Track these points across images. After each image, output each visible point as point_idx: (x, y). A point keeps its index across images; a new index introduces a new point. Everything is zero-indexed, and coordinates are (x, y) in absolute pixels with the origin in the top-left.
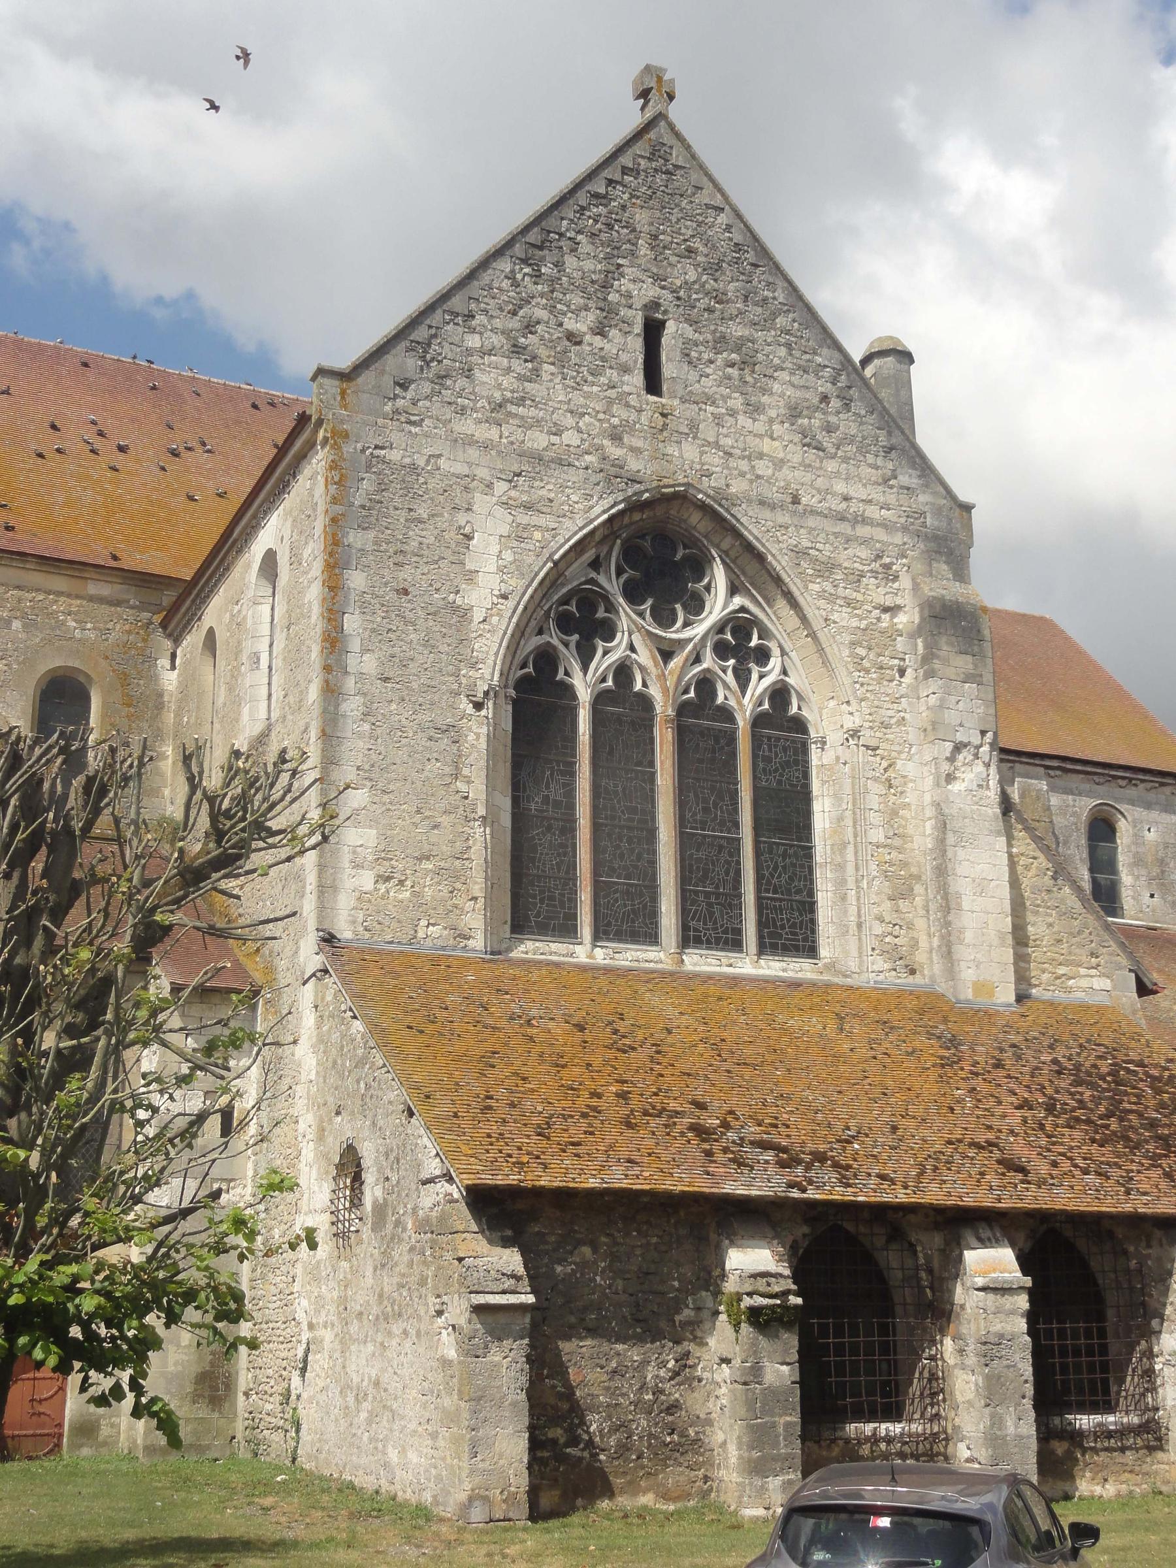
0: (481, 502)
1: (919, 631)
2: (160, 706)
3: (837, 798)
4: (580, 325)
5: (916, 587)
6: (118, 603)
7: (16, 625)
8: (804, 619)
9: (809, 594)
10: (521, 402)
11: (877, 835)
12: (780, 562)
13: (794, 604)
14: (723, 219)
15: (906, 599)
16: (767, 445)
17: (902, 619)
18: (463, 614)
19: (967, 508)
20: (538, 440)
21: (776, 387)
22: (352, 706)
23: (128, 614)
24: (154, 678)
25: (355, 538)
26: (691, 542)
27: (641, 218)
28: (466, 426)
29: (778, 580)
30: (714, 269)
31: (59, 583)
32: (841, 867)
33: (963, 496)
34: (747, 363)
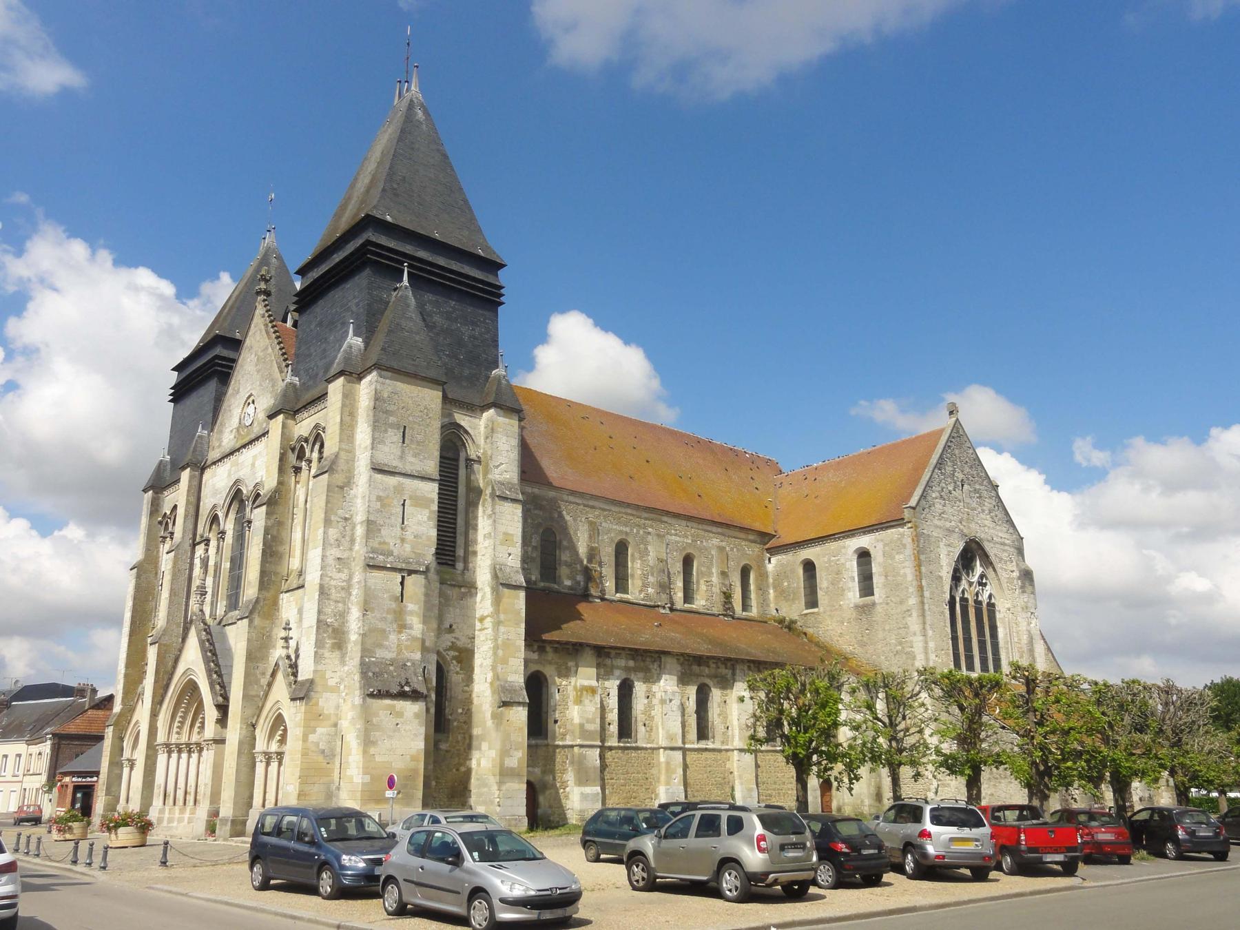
0: (942, 545)
1: (1019, 578)
2: (767, 577)
3: (1005, 628)
4: (951, 488)
5: (1017, 565)
6: (754, 542)
7: (735, 550)
8: (997, 575)
9: (998, 566)
10: (943, 513)
11: (1016, 640)
12: (993, 558)
13: (995, 570)
14: (971, 451)
15: (1015, 569)
16: (986, 522)
17: (1014, 574)
18: (941, 577)
19: (1022, 538)
20: (948, 525)
21: (986, 504)
22: (926, 607)
23: (758, 546)
24: (765, 567)
25: (922, 557)
26: (972, 552)
27: (957, 452)
28: (937, 522)
29: (991, 563)
30: (971, 467)
31: (742, 535)
32: (1007, 648)
33: (1022, 536)
34: (980, 497)
